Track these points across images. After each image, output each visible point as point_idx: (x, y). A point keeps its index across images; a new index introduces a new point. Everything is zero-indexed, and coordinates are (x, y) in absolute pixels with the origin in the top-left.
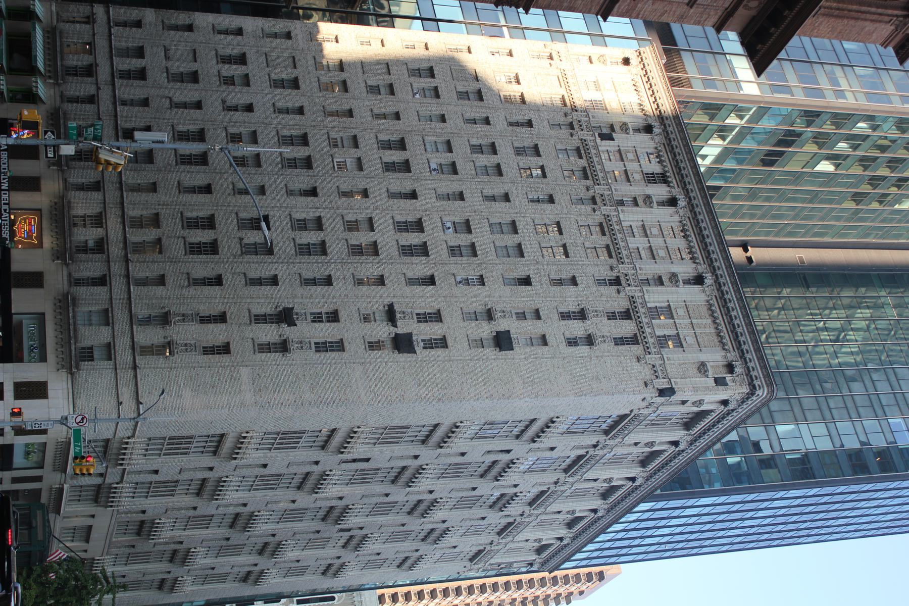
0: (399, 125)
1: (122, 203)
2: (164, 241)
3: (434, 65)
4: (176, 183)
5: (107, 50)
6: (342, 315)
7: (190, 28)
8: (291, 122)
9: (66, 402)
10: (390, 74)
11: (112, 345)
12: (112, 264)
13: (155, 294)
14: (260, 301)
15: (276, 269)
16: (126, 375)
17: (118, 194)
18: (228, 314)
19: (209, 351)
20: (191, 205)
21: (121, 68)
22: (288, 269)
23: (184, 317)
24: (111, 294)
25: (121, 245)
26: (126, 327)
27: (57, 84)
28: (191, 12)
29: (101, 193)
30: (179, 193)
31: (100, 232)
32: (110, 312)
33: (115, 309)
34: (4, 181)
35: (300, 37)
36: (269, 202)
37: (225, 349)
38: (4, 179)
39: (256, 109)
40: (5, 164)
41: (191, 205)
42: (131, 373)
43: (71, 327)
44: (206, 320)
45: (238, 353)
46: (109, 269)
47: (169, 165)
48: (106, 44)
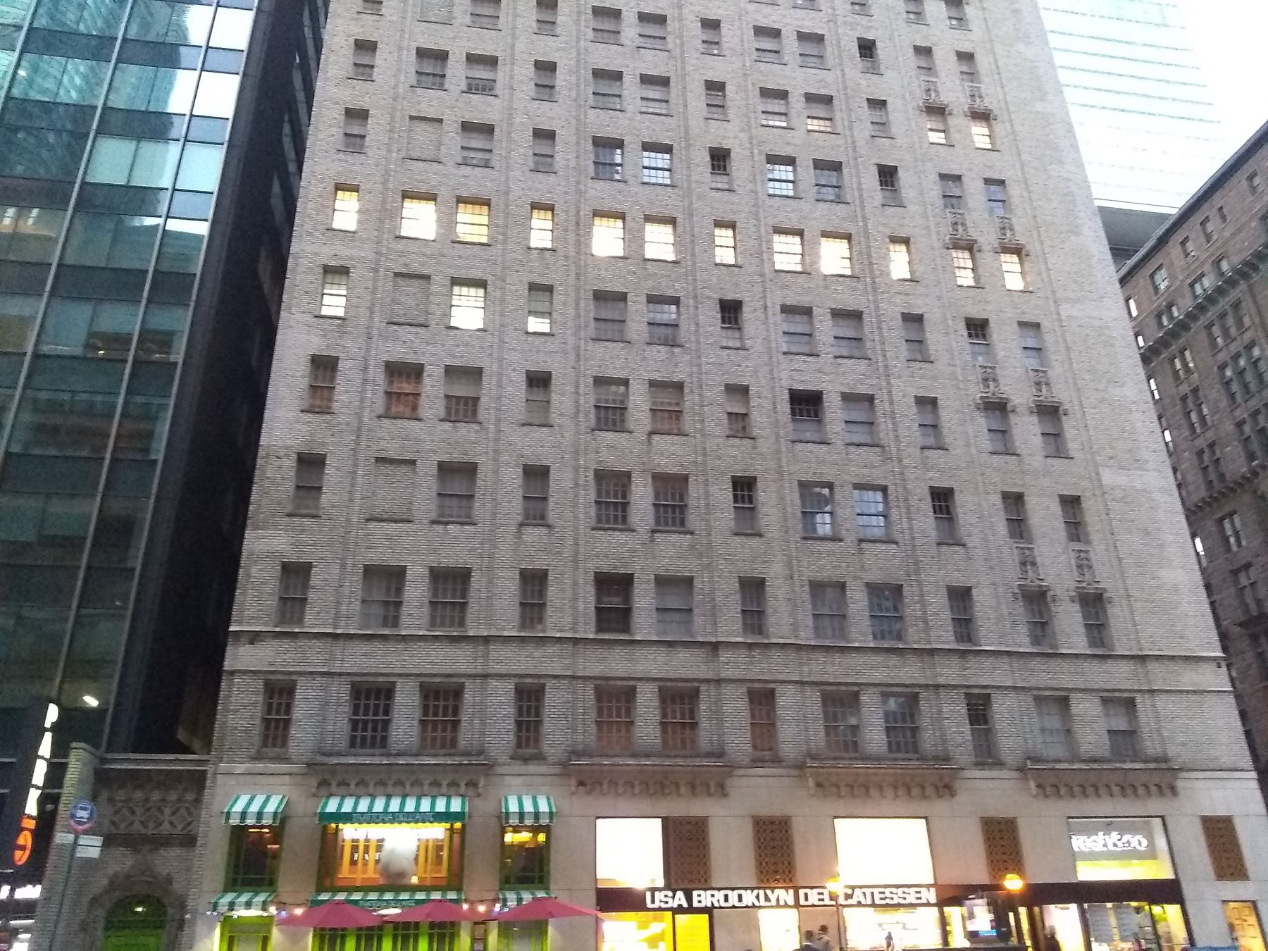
0: (565, 135)
1: (799, 647)
2: (875, 576)
3: (414, 45)
4: (738, 539)
5: (378, 648)
6: (976, 312)
7: (311, 463)
8: (571, 311)
9: (1231, 784)
10: (441, 121)
11: (1105, 694)
12: (941, 681)
13: (990, 607)
14: (970, 431)
15: (904, 396)
16: (1160, 676)
17: (776, 654)
18: (1006, 489)
19: (1076, 528)
20: (785, 519)
21: (426, 620)
22: (900, 377)
23: (1027, 562)
24: (1006, 688)
25: (894, 660)
26: (1065, 665)
27: (489, 768)
28: (261, 452)
29: (780, 690)
30: (761, 535)
31: (869, 699)
32: (1042, 693)
33: (1033, 682)
34: (773, 897)
35: (347, 252)
36: (763, 382)
37: (1071, 503)
38: (767, 899)
39: (541, 367)
40: (726, 900)
41: (785, 519)
42: (1152, 666)
43: (1095, 766)
44: (1018, 526)
45: (1075, 484)
46: (955, 687)
47: (692, 547)
48: (361, 648)
